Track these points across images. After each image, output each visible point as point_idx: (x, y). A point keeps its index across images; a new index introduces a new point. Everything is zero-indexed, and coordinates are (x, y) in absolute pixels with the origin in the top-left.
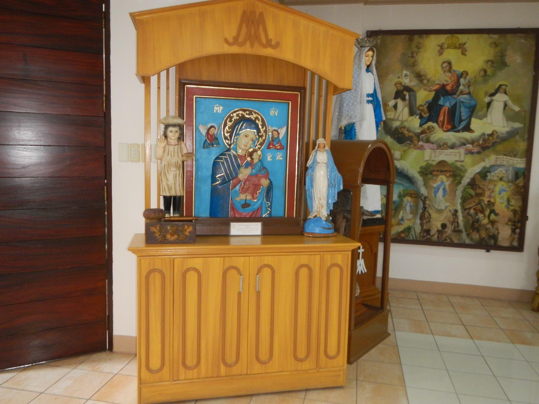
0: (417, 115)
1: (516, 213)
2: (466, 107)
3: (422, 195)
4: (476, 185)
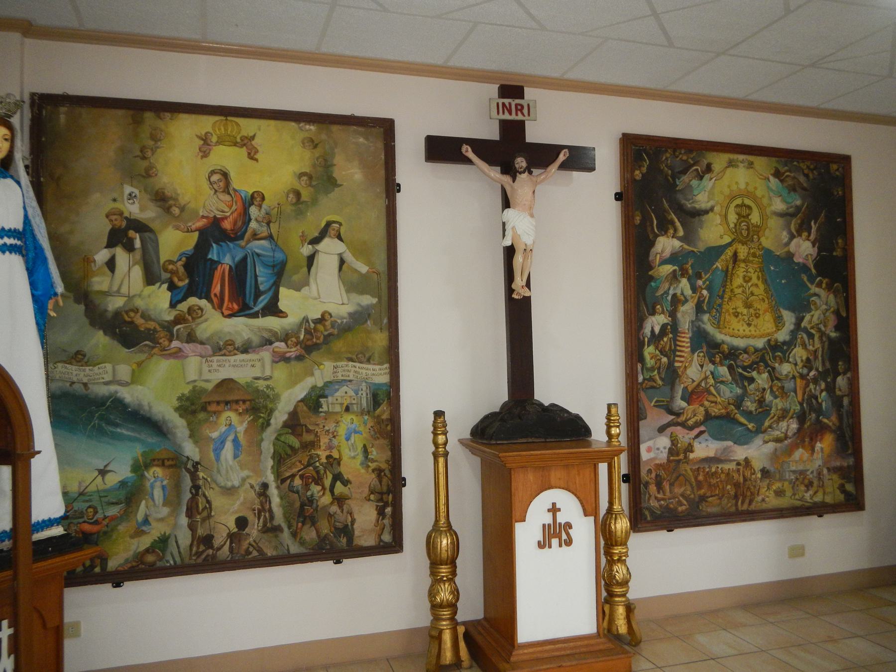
0: (163, 283)
1: (383, 474)
2: (265, 265)
3: (188, 458)
4: (303, 425)
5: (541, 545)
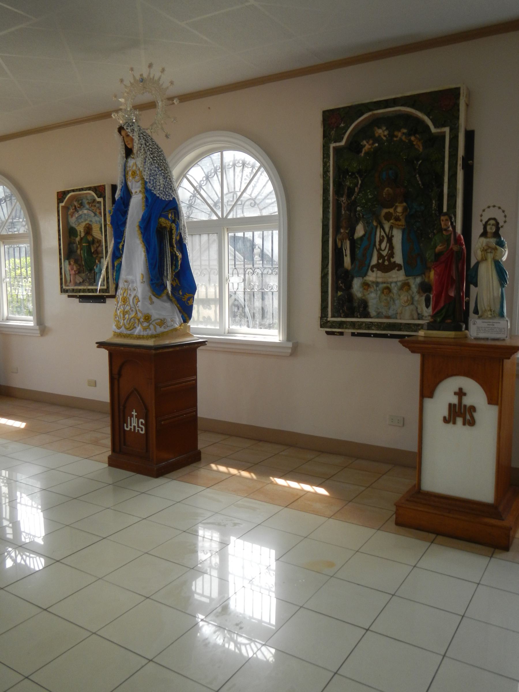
5: (446, 420)
